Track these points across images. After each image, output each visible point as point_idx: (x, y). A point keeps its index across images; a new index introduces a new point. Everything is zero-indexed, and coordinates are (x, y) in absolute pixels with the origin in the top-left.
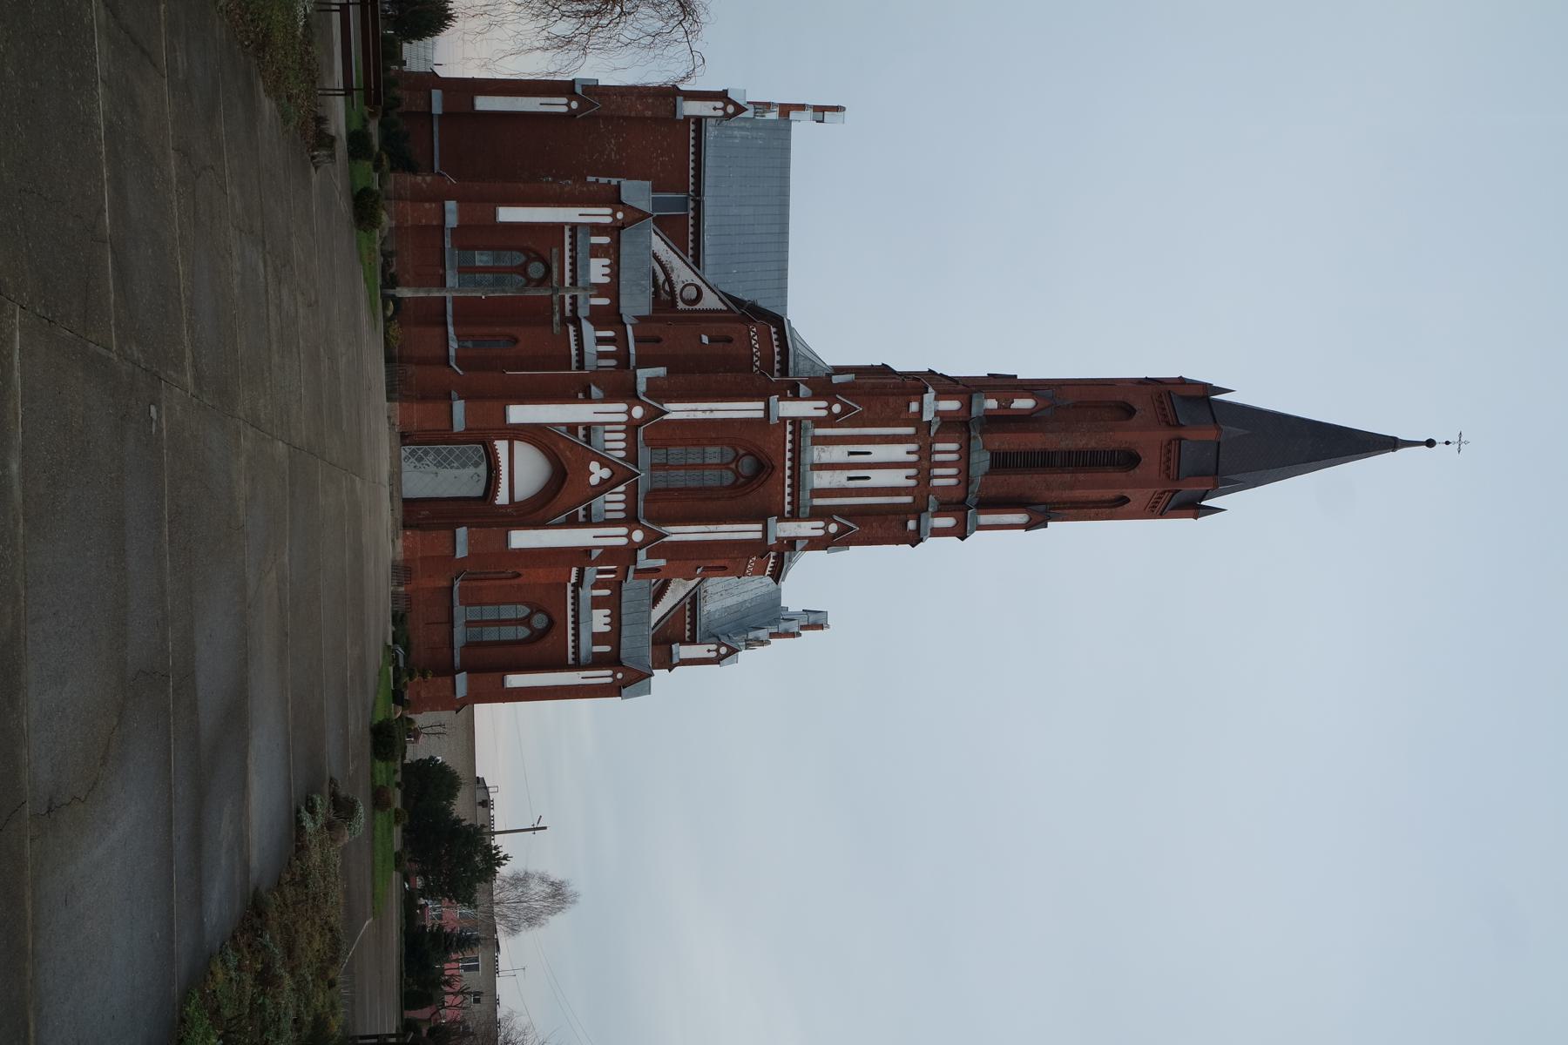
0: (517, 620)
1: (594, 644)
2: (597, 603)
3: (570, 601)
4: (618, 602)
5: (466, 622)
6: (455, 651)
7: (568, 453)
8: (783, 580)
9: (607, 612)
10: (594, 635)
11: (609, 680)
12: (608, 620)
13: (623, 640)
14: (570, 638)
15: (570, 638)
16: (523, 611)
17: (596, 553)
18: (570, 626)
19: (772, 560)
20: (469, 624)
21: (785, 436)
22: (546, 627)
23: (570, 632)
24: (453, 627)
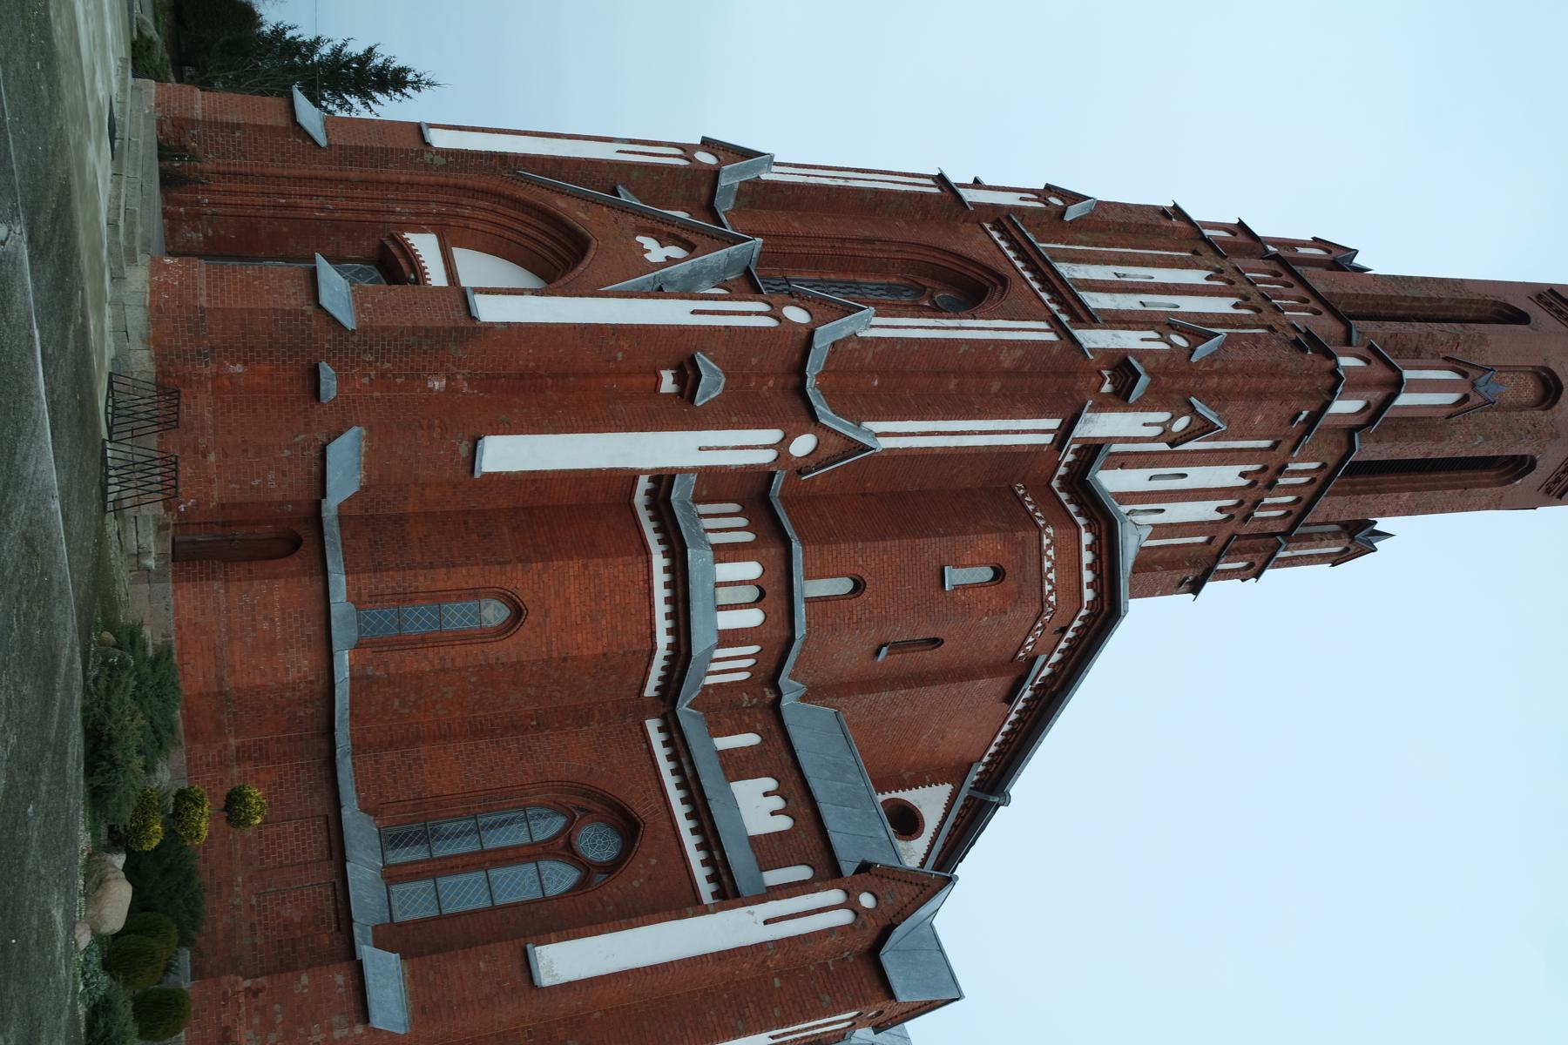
0: (533, 845)
1: (766, 864)
2: (738, 766)
3: (665, 767)
4: (785, 755)
5: (384, 867)
6: (356, 931)
7: (581, 215)
8: (1126, 612)
9: (770, 783)
10: (755, 842)
11: (844, 917)
12: (777, 803)
13: (835, 839)
14: (695, 857)
15: (695, 857)
16: (548, 827)
17: (711, 385)
18: (685, 826)
19: (1086, 538)
20: (392, 876)
21: (998, 245)
22: (618, 857)
23: (690, 842)
24: (343, 860)
